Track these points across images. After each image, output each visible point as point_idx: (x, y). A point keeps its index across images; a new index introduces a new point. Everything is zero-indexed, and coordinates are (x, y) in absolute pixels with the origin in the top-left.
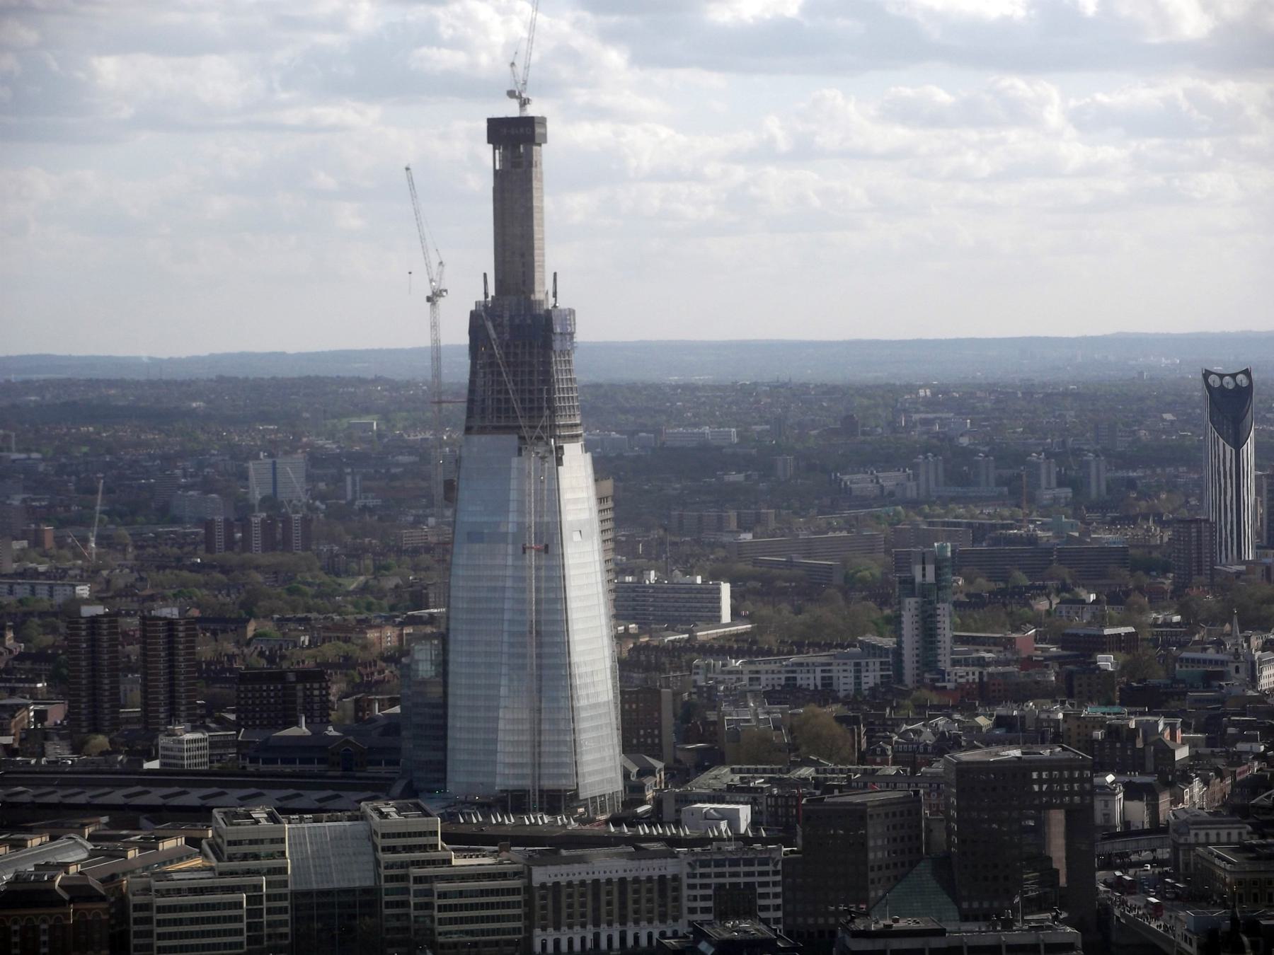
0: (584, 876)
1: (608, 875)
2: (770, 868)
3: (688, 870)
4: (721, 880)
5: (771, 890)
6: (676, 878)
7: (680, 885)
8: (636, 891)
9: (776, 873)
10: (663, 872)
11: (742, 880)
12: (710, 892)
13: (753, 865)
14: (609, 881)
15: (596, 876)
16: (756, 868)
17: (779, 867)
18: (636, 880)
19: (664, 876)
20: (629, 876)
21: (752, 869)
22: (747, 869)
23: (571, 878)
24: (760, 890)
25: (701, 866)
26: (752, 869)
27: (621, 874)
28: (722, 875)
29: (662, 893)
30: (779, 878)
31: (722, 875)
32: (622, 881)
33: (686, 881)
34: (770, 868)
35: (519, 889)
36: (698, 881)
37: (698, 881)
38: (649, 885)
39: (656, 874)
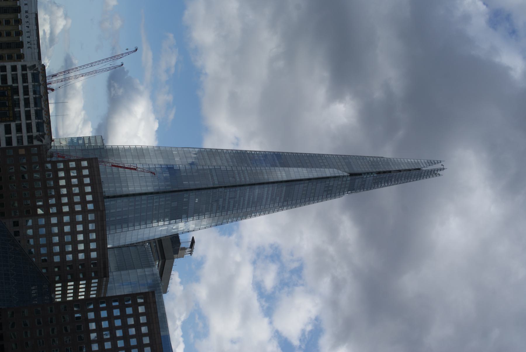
2: (35, 132)
3: (29, 64)
4: (21, 91)
5: (14, 135)
6: (20, 57)
7: (15, 61)
8: (8, 22)
9: (30, 139)
10: (26, 45)
11: (22, 109)
12: (10, 82)
16: (34, 121)
18: (18, 22)
19: (22, 47)
20: (22, 16)
22: (33, 112)
24: (13, 125)
25: (33, 75)
26: (33, 117)
27: (24, 9)
28: (26, 92)
29: (8, 45)
31: (26, 92)
32: (18, 10)
33: (19, 65)
34: (35, 132)
36: (19, 71)
37: (19, 71)
38: (13, 33)
39: (24, 39)
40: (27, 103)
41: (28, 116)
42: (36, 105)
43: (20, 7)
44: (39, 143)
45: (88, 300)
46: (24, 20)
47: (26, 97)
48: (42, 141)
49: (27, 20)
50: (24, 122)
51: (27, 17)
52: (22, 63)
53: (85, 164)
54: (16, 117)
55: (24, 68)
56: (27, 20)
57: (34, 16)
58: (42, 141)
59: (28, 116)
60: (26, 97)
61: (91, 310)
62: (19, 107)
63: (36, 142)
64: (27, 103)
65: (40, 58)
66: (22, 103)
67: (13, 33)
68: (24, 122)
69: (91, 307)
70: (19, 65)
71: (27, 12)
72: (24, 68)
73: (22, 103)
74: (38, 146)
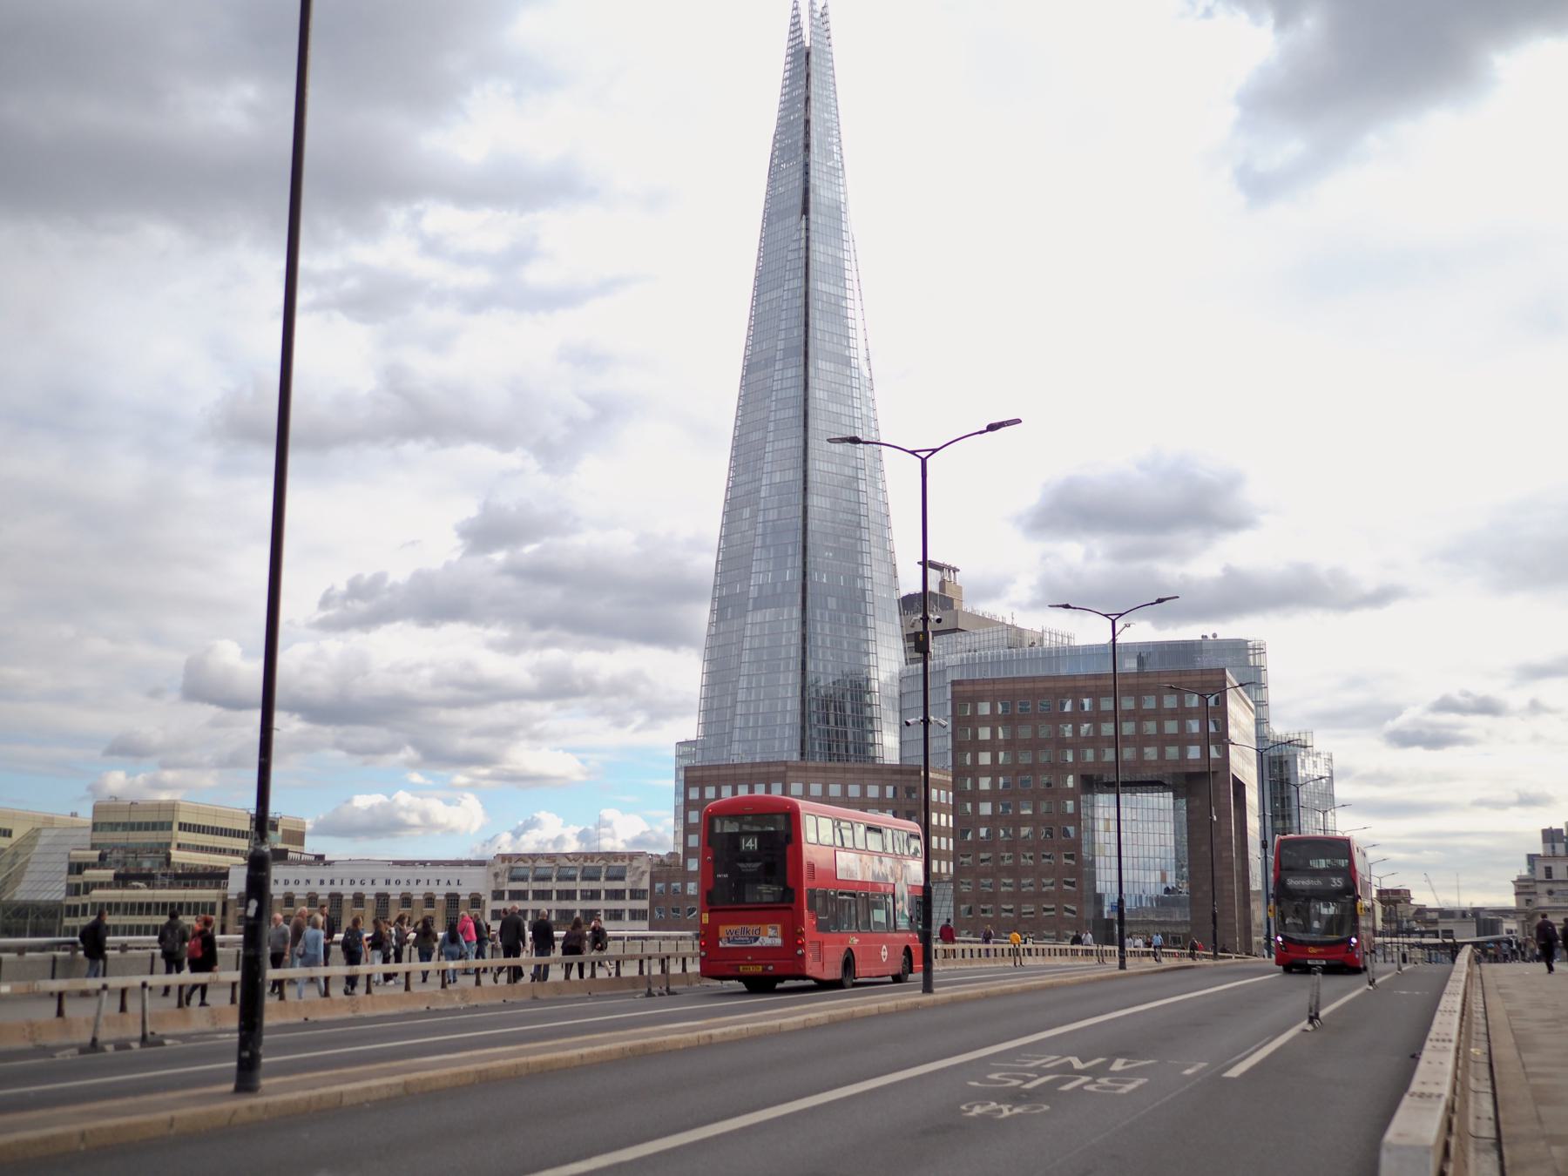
0: (314, 887)
1: (357, 888)
6: (476, 901)
7: (483, 913)
9: (636, 894)
10: (453, 889)
13: (597, 879)
14: (359, 899)
15: (337, 888)
17: (645, 884)
18: (406, 900)
21: (594, 885)
23: (291, 888)
26: (594, 885)
27: (381, 887)
30: (643, 905)
32: (383, 899)
33: (491, 905)
35: (213, 905)
40: (569, 895)
41: (594, 895)
42: (573, 878)
43: (378, 895)
44: (647, 878)
45: (956, 810)
46: (403, 888)
47: (554, 895)
48: (643, 873)
49: (403, 883)
50: (602, 905)
51: (398, 882)
52: (487, 898)
53: (694, 794)
54: (591, 914)
55: (498, 895)
56: (403, 883)
57: (398, 869)
58: (643, 873)
59: (594, 895)
60: (554, 895)
61: (976, 808)
62: (573, 911)
63: (645, 884)
64: (569, 895)
65: (481, 863)
66: (566, 905)
67: (428, 911)
68: (602, 905)
69: (969, 806)
70: (491, 905)
71: (388, 882)
72: (498, 895)
73: (566, 905)
74: (654, 879)
